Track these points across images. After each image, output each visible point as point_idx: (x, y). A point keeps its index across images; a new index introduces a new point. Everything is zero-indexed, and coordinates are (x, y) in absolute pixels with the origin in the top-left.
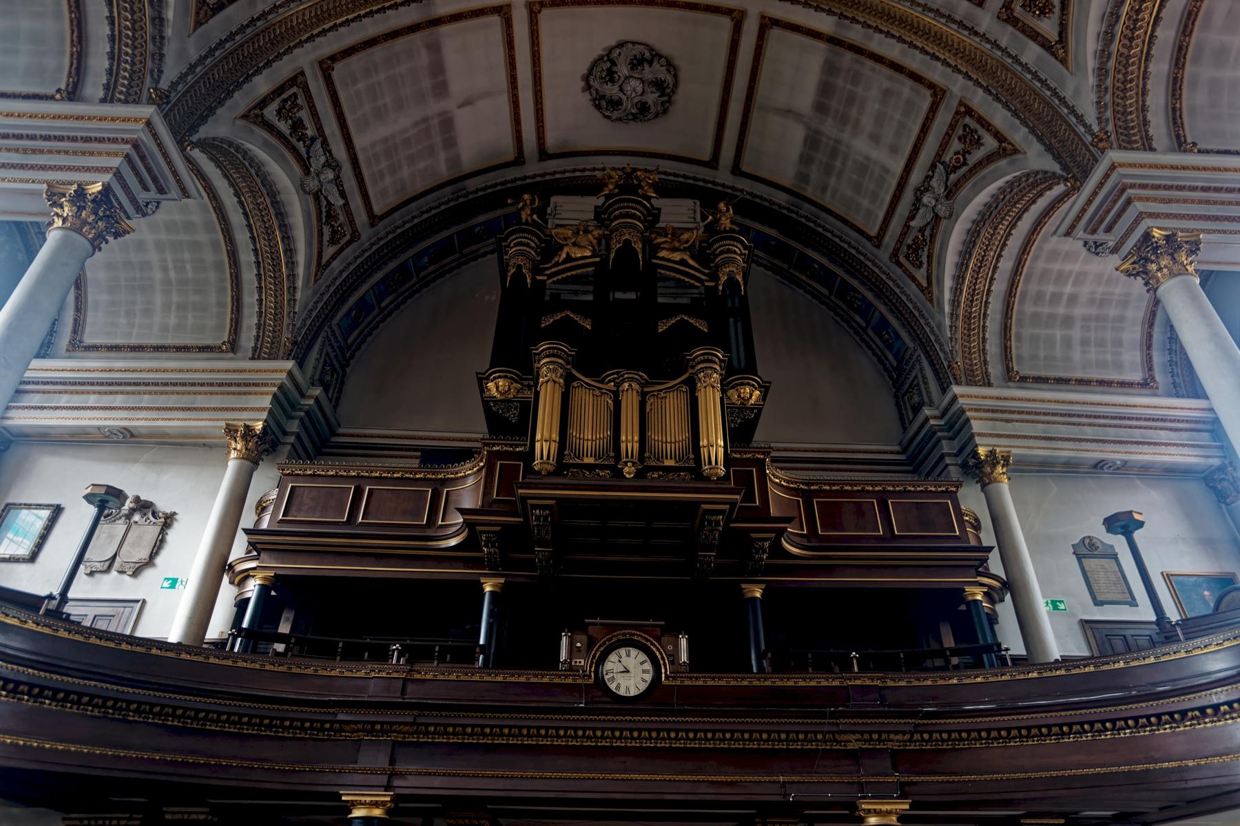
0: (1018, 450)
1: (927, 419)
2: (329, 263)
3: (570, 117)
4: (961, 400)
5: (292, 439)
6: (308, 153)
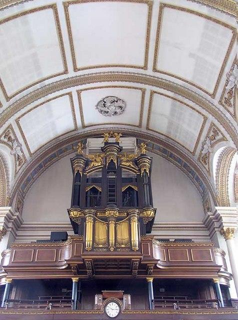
1: (209, 216)
3: (93, 117)
4: (218, 212)
5: (10, 229)
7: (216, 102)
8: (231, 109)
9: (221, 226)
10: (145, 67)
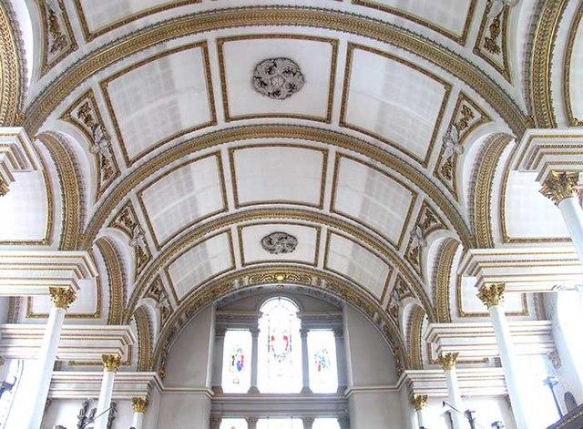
0: (430, 394)
3: (255, 253)
7: (401, 254)
8: (418, 267)
9: (411, 392)
10: (321, 207)
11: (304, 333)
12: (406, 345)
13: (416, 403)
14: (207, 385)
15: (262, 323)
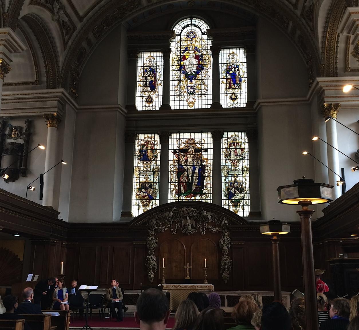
2: (68, 42)
4: (320, 84)
6: (53, 7)
9: (322, 101)
11: (215, 52)
12: (320, 50)
13: (325, 113)
14: (120, 100)
15: (174, 46)
